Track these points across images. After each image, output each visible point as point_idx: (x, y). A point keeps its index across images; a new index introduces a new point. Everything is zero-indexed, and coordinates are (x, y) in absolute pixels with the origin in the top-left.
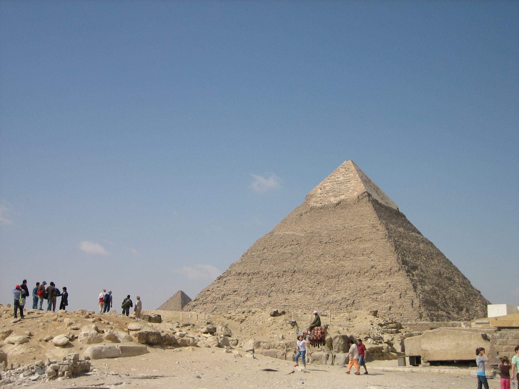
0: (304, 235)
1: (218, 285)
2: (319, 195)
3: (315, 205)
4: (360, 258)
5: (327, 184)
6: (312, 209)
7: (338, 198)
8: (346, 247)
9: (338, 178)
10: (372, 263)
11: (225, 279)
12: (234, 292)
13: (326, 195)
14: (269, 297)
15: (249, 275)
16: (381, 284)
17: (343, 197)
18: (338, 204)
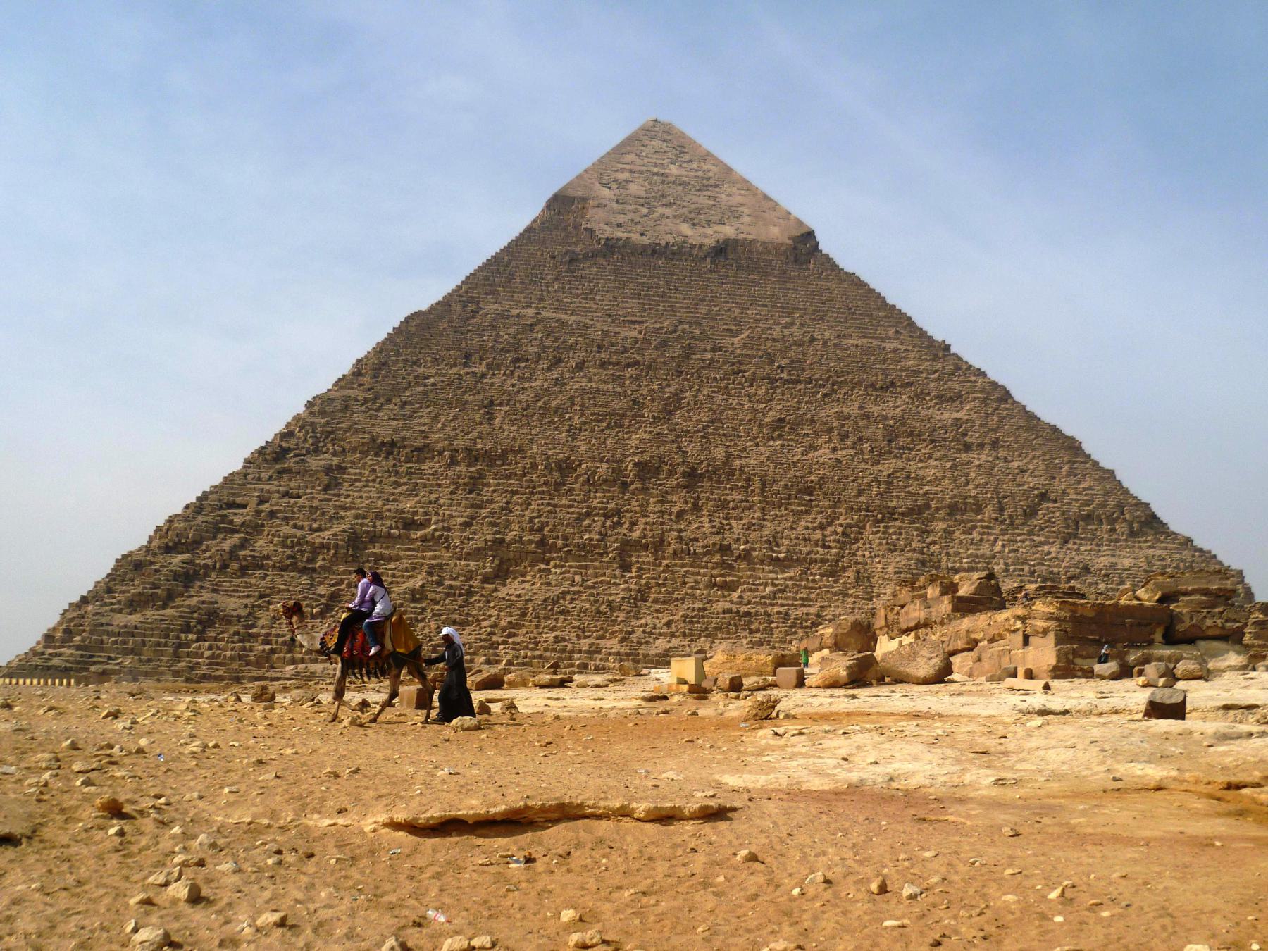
0: (634, 334)
1: (284, 484)
2: (615, 206)
3: (620, 233)
4: (964, 456)
5: (621, 176)
6: (611, 246)
7: (709, 231)
8: (875, 410)
9: (656, 165)
10: (1031, 481)
11: (315, 463)
12: (410, 525)
13: (645, 210)
14: (626, 567)
15: (453, 462)
16: (1127, 562)
17: (728, 231)
18: (722, 250)
